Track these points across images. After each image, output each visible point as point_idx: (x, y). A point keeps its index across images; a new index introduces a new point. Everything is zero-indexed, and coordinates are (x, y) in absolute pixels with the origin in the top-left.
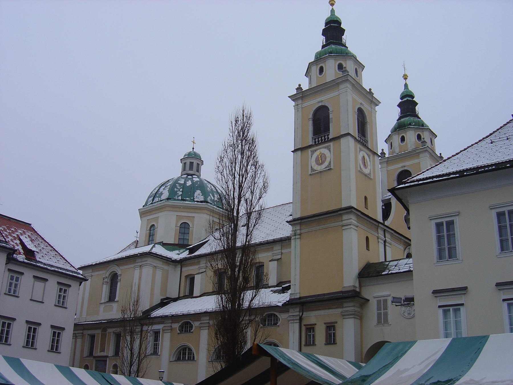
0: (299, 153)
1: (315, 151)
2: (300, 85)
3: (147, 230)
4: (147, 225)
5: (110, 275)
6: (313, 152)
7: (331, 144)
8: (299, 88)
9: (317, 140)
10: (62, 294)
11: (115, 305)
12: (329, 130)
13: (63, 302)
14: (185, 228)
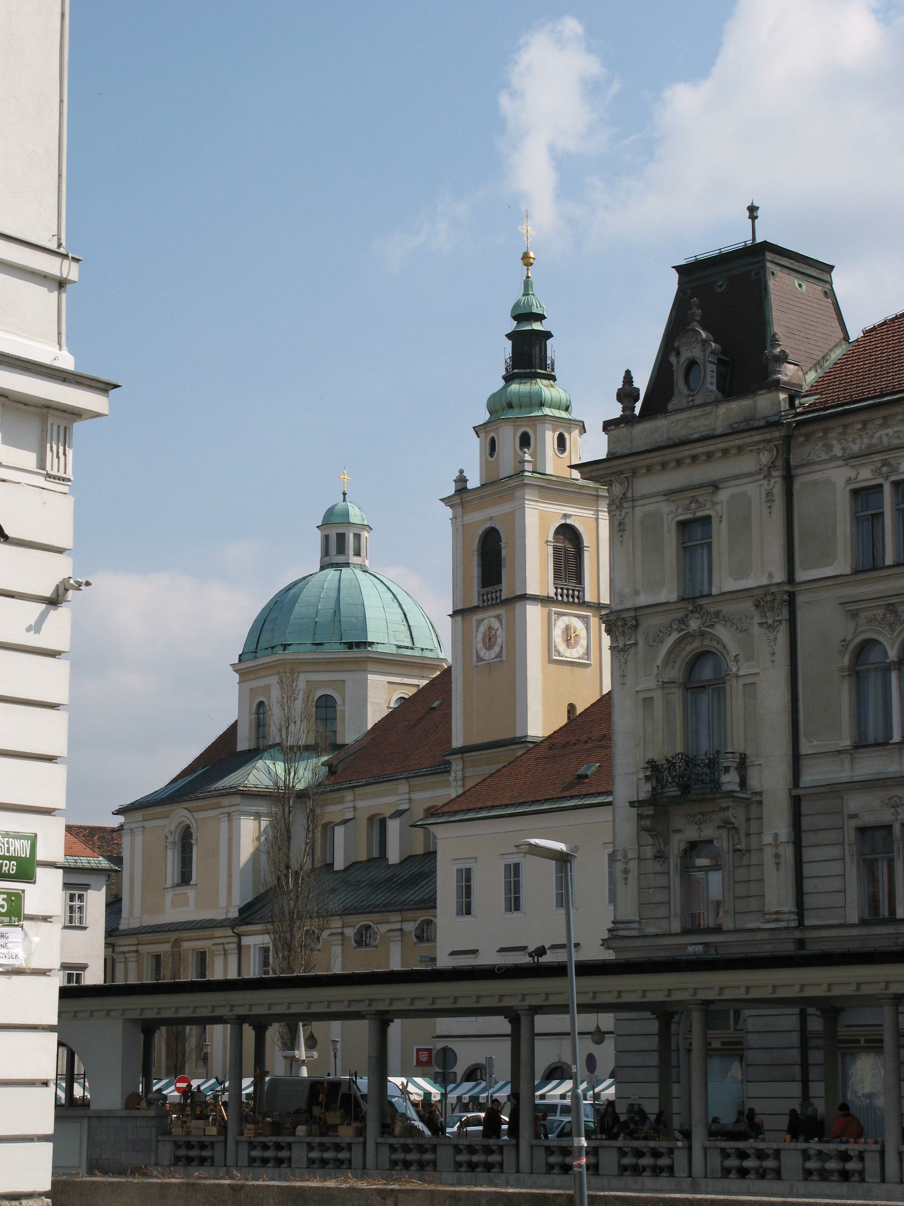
0: (459, 619)
1: (483, 620)
2: (461, 472)
3: (251, 714)
4: (251, 702)
5: (177, 828)
6: (480, 622)
7: (501, 611)
8: (461, 480)
9: (485, 597)
10: (77, 903)
11: (190, 892)
12: (501, 583)
13: (81, 918)
14: (326, 707)
